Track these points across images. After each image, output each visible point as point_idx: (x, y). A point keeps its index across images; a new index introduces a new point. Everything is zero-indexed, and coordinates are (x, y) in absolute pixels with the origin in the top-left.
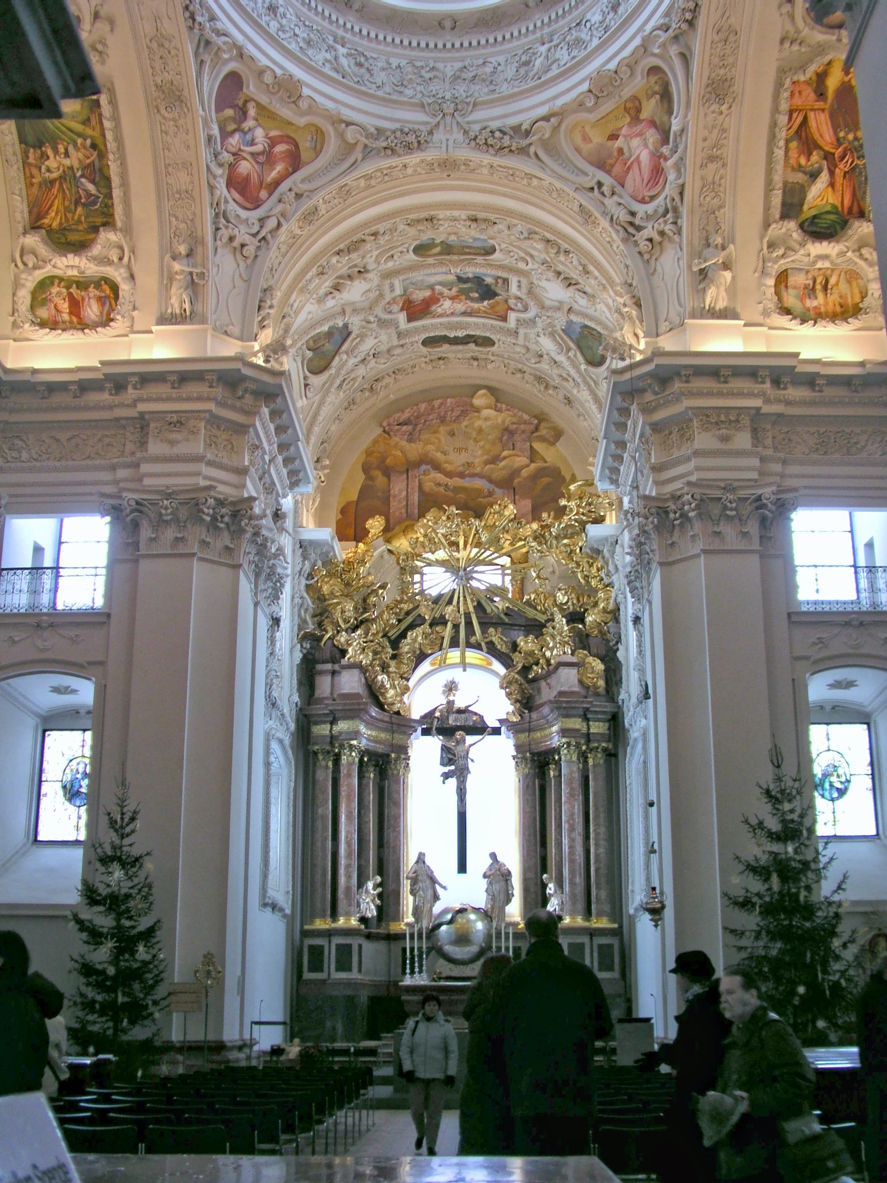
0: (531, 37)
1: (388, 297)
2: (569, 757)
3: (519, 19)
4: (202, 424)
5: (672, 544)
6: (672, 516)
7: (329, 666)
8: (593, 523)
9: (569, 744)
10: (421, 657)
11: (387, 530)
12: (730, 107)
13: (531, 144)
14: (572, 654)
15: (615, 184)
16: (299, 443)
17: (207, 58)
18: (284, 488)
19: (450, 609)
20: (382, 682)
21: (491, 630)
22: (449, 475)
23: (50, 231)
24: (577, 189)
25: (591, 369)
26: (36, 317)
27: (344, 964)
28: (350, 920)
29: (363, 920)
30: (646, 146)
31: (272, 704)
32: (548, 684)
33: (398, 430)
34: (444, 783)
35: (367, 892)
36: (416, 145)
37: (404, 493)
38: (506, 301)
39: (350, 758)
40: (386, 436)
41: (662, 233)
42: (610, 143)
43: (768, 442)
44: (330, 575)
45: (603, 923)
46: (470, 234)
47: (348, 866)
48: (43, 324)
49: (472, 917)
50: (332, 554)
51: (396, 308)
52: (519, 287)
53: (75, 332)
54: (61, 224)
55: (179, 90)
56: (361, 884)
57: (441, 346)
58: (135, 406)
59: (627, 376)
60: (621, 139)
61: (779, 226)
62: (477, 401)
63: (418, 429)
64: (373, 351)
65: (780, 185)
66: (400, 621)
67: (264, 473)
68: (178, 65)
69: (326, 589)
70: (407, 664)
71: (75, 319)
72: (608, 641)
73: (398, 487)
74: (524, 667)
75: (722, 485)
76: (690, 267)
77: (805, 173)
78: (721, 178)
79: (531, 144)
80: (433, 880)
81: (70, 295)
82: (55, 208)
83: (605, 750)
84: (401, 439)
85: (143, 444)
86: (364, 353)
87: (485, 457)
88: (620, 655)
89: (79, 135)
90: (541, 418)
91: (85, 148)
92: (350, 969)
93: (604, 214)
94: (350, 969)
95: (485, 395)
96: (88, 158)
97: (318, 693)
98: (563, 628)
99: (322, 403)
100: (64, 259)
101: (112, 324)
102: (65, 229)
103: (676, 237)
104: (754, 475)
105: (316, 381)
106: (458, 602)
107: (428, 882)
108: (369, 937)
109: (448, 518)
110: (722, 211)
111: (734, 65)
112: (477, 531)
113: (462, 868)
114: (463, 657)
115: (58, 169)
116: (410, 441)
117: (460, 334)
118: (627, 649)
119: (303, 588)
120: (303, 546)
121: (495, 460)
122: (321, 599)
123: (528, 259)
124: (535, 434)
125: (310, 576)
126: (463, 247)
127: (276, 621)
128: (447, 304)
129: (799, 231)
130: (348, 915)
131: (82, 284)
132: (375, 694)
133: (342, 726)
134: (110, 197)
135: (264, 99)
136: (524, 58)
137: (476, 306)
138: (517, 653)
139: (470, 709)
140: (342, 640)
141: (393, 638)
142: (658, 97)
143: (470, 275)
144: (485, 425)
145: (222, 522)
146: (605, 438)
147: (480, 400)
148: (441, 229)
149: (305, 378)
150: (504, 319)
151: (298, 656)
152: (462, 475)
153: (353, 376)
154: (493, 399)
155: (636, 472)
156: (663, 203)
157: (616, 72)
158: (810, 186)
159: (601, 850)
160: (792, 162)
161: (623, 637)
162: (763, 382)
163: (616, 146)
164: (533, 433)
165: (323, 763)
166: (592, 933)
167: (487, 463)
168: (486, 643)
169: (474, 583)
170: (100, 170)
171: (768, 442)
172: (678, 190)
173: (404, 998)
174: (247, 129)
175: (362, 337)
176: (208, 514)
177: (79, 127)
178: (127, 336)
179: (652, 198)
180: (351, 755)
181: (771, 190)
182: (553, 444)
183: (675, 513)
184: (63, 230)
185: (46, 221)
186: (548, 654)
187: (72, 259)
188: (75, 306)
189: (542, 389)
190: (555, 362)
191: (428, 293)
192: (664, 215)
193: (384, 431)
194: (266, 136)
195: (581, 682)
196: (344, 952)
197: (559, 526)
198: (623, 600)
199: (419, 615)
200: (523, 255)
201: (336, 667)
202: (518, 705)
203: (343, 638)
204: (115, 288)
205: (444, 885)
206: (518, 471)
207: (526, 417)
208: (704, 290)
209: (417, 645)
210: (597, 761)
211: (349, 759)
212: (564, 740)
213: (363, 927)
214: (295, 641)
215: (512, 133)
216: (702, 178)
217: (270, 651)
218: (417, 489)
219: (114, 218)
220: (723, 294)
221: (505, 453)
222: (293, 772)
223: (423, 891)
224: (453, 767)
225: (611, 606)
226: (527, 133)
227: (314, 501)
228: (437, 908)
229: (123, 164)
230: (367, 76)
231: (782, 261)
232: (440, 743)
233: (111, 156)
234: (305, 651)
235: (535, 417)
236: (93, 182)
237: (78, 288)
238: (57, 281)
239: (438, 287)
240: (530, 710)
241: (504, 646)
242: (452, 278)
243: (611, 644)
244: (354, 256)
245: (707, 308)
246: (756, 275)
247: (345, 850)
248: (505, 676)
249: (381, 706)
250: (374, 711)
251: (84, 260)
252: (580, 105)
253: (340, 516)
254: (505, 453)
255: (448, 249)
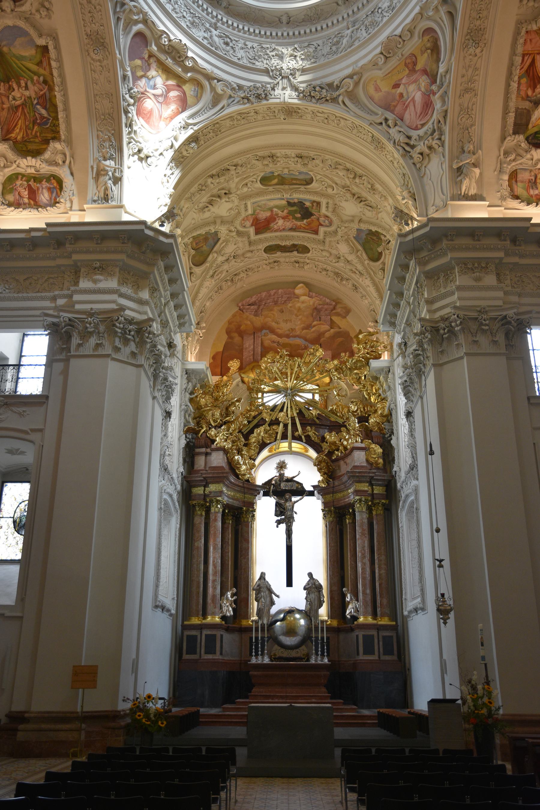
0: (341, 26)
1: (243, 215)
2: (360, 509)
3: (332, 14)
4: (117, 270)
5: (442, 352)
6: (442, 332)
7: (203, 450)
8: (373, 359)
9: (360, 500)
10: (262, 446)
11: (241, 369)
12: (482, 51)
13: (339, 95)
14: (362, 442)
15: (397, 118)
16: (185, 293)
17: (122, 16)
18: (174, 327)
19: (282, 414)
20: (238, 460)
21: (309, 428)
22: (280, 336)
23: (15, 142)
24: (371, 124)
25: (372, 263)
26: (5, 200)
27: (210, 649)
28: (215, 618)
29: (224, 618)
30: (419, 89)
31: (165, 469)
32: (345, 462)
33: (248, 309)
34: (277, 527)
35: (227, 599)
36: (263, 96)
37: (252, 347)
38: (318, 219)
39: (217, 509)
40: (241, 312)
41: (430, 148)
42: (394, 91)
43: (508, 282)
44: (204, 393)
45: (385, 621)
46: (297, 167)
47: (214, 581)
48: (10, 205)
49: (297, 616)
50: (206, 380)
51: (248, 224)
52: (327, 207)
53: (32, 210)
54: (23, 137)
55: (103, 39)
56: (223, 594)
57: (276, 253)
58: (71, 257)
59: (410, 237)
60: (402, 86)
61: (512, 139)
62: (297, 291)
63: (261, 308)
64: (233, 254)
65: (514, 110)
66: (249, 422)
67: (161, 313)
68: (102, 19)
69: (203, 401)
70: (254, 450)
71: (32, 202)
72: (384, 434)
73: (248, 343)
74: (329, 452)
75: (479, 309)
76: (451, 167)
77: (530, 101)
78: (473, 104)
79: (339, 95)
80: (271, 591)
81: (29, 186)
82: (19, 126)
83: (384, 505)
84: (250, 314)
85: (76, 283)
86: (228, 255)
87: (302, 325)
88: (393, 442)
89: (35, 73)
90: (337, 301)
91: (38, 82)
92: (215, 653)
93: (389, 139)
94: (215, 653)
95: (302, 287)
96: (42, 90)
97: (196, 467)
98: (355, 425)
99: (201, 285)
100: (25, 160)
101: (57, 205)
102: (26, 141)
103: (440, 149)
104: (500, 303)
105: (198, 270)
106: (287, 410)
107: (267, 592)
108: (228, 630)
109: (281, 357)
110: (474, 127)
111: (487, 17)
112: (299, 365)
113: (289, 583)
114: (290, 447)
115: (21, 97)
116: (256, 315)
117: (288, 243)
118: (398, 438)
119: (187, 399)
120: (189, 374)
121: (308, 327)
122: (198, 408)
123: (334, 185)
124: (334, 311)
125: (191, 393)
126: (292, 179)
127: (168, 414)
128: (280, 222)
129: (526, 142)
130: (213, 614)
131: (38, 179)
132: (233, 467)
133: (213, 487)
134: (56, 118)
135: (162, 57)
136: (335, 40)
137: (299, 223)
138: (325, 443)
139: (294, 479)
140: (213, 433)
141: (245, 433)
142: (429, 51)
143: (296, 201)
144: (302, 306)
145: (129, 335)
146: (389, 290)
148: (278, 164)
149: (190, 268)
150: (316, 232)
151: (183, 442)
152: (288, 336)
153: (221, 270)
154: (307, 290)
155: (409, 313)
156: (431, 126)
157: (400, 36)
158: (533, 111)
159: (383, 572)
160: (523, 93)
161: (395, 431)
162: (505, 240)
163: (398, 92)
164: (332, 311)
165: (199, 513)
166: (379, 628)
167: (303, 329)
168: (305, 436)
169: (298, 399)
170: (50, 99)
171: (508, 282)
172: (443, 114)
173: (251, 673)
174: (150, 77)
175: (227, 241)
176: (120, 328)
177: (34, 68)
178: (67, 213)
179: (423, 125)
180: (217, 507)
181: (507, 114)
182: (345, 317)
183: (444, 329)
184: (24, 142)
185: (13, 135)
186: (345, 443)
187: (30, 161)
188: (33, 194)
189: (339, 281)
190: (348, 261)
191: (268, 214)
192: (432, 134)
193: (240, 309)
194: (164, 84)
195: (367, 461)
196: (211, 639)
197: (352, 361)
198: (394, 407)
199: (262, 419)
200: (330, 183)
201: (209, 450)
202: (326, 476)
203: (213, 432)
204: (60, 182)
205: (278, 594)
206: (323, 333)
207: (328, 301)
208: (461, 182)
209: (260, 438)
210: (379, 512)
211: (217, 509)
212: (357, 498)
213: (224, 622)
214: (182, 433)
215: (327, 88)
216: (460, 105)
217: (164, 434)
218: (260, 344)
219: (60, 135)
220: (474, 184)
221: (315, 323)
222: (179, 517)
223: (264, 599)
224: (283, 517)
225: (386, 412)
226: (338, 87)
227: (195, 348)
228: (274, 610)
229: (65, 95)
230: (231, 52)
231: (514, 164)
232: (275, 501)
233: (57, 88)
234: (188, 440)
235: (334, 301)
236: (45, 108)
237: (35, 181)
238: (20, 177)
239: (275, 209)
240: (334, 479)
241: (316, 439)
242: (284, 202)
243: (386, 436)
244: (222, 179)
245: (463, 194)
246: (496, 173)
247: (212, 570)
248: (317, 458)
249: (237, 476)
250: (232, 479)
251: (39, 162)
252: (374, 64)
253: (212, 361)
254: (315, 323)
255: (282, 181)
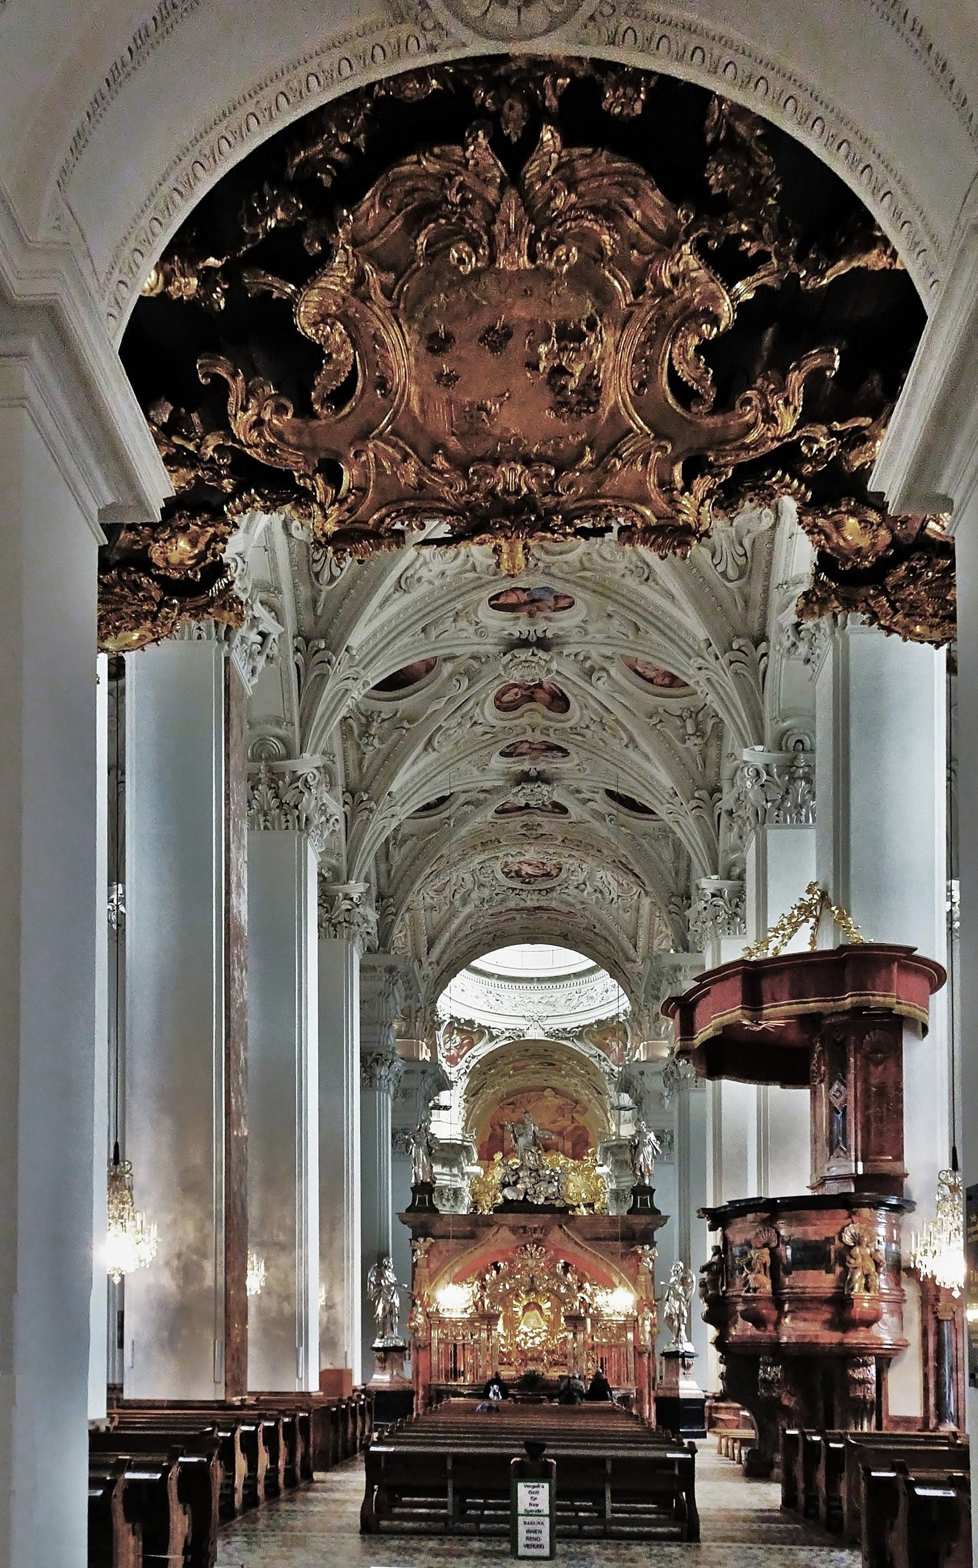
62: (545, 1093)
121: (554, 1122)
147: (548, 1092)
